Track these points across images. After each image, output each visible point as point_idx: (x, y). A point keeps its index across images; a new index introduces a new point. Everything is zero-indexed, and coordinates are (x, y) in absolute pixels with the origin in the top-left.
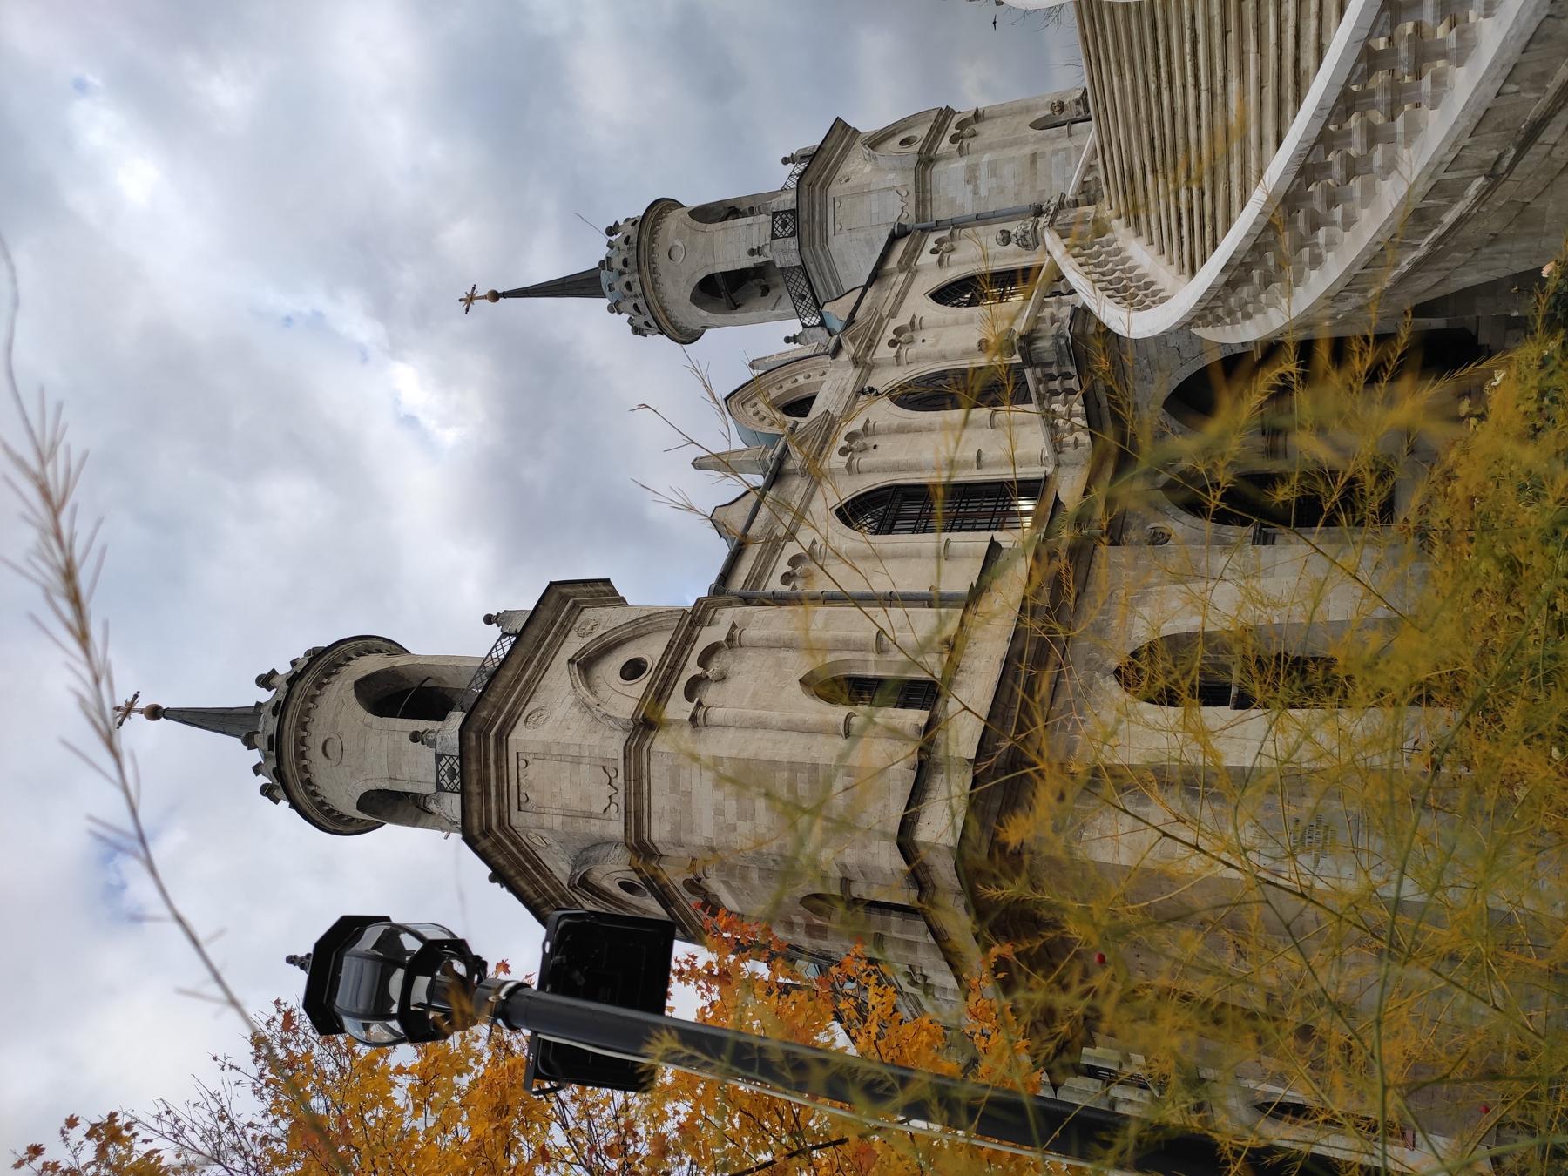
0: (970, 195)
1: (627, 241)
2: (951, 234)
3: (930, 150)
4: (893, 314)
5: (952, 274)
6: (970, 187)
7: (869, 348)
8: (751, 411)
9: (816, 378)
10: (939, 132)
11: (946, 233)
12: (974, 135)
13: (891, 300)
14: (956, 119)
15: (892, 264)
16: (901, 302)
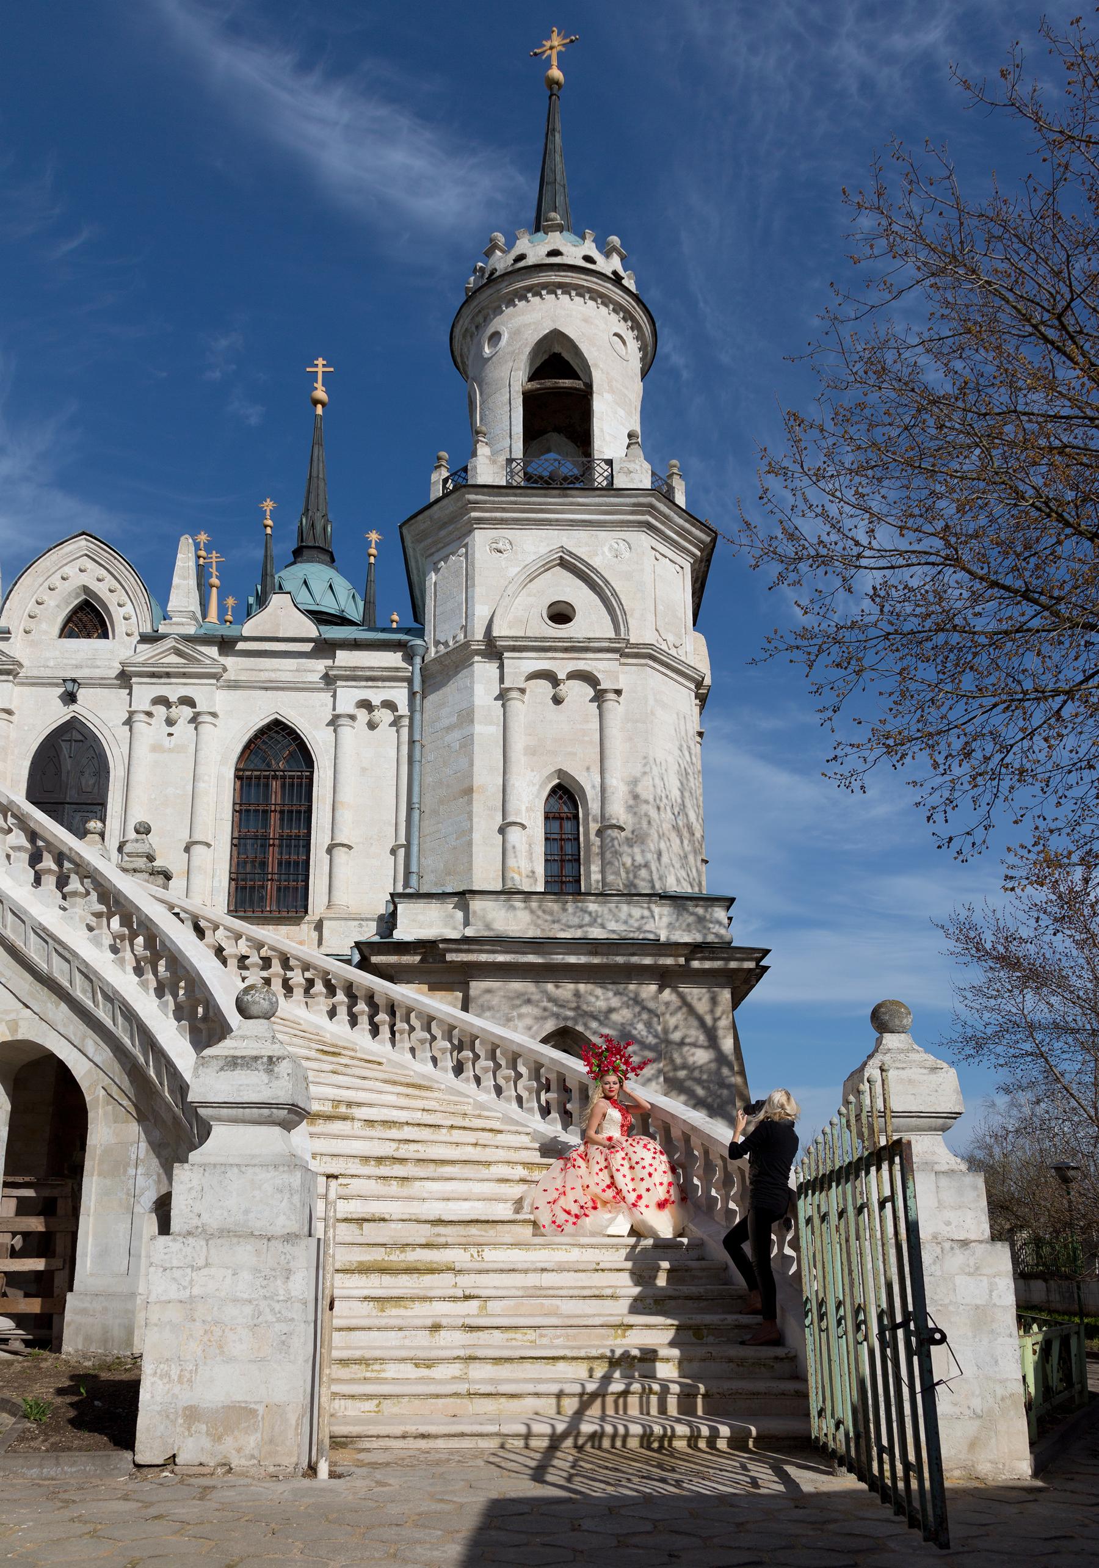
0: (446, 722)
1: (521, 257)
2: (401, 717)
3: (514, 649)
4: (234, 685)
5: (318, 739)
6: (454, 719)
7: (153, 675)
8: (68, 570)
9: (120, 627)
10: (566, 650)
11: (403, 709)
12: (557, 700)
13: (264, 676)
14: (601, 666)
15: (344, 658)
16: (266, 689)
